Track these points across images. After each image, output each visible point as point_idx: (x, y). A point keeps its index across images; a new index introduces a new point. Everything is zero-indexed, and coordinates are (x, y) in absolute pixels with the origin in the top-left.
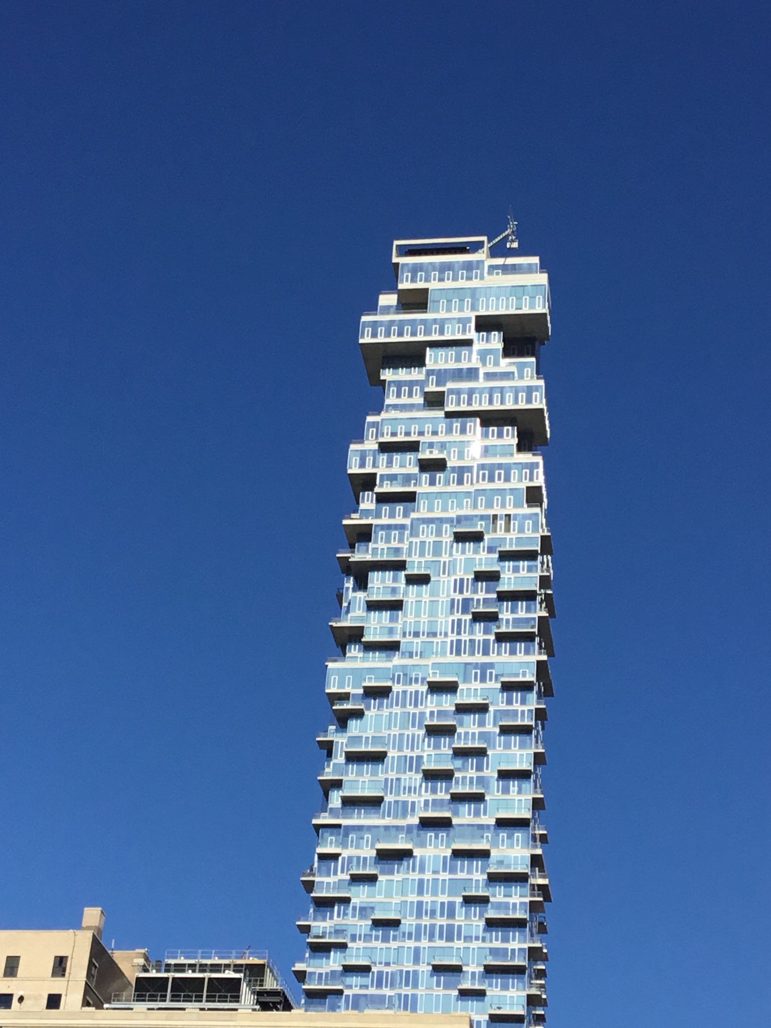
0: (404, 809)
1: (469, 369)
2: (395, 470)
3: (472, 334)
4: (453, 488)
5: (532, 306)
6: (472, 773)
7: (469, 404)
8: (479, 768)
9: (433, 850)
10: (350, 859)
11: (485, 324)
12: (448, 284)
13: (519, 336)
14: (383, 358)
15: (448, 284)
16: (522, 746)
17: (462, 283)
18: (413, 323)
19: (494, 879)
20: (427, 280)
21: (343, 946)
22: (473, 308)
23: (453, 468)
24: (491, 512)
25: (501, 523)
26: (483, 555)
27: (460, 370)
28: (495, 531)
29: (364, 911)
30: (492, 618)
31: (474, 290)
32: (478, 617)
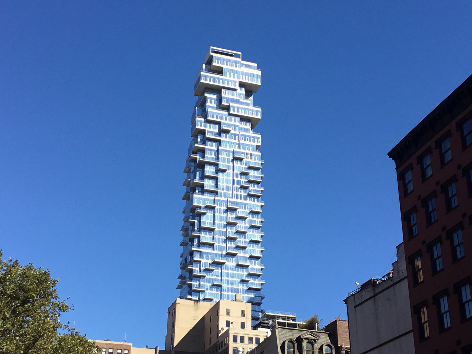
0: (220, 248)
1: (237, 100)
2: (212, 130)
3: (237, 87)
4: (232, 140)
5: (257, 82)
6: (242, 239)
7: (238, 112)
8: (245, 238)
9: (230, 263)
10: (205, 263)
11: (242, 85)
12: (229, 67)
13: (250, 90)
15: (229, 67)
16: (257, 233)
17: (233, 68)
18: (218, 79)
19: (250, 275)
20: (223, 64)
21: (204, 291)
22: (238, 78)
23: (232, 134)
24: (245, 151)
25: (249, 156)
26: (244, 166)
27: (233, 99)
28: (247, 158)
29: (210, 280)
30: (246, 188)
31: (237, 71)
32: (242, 187)
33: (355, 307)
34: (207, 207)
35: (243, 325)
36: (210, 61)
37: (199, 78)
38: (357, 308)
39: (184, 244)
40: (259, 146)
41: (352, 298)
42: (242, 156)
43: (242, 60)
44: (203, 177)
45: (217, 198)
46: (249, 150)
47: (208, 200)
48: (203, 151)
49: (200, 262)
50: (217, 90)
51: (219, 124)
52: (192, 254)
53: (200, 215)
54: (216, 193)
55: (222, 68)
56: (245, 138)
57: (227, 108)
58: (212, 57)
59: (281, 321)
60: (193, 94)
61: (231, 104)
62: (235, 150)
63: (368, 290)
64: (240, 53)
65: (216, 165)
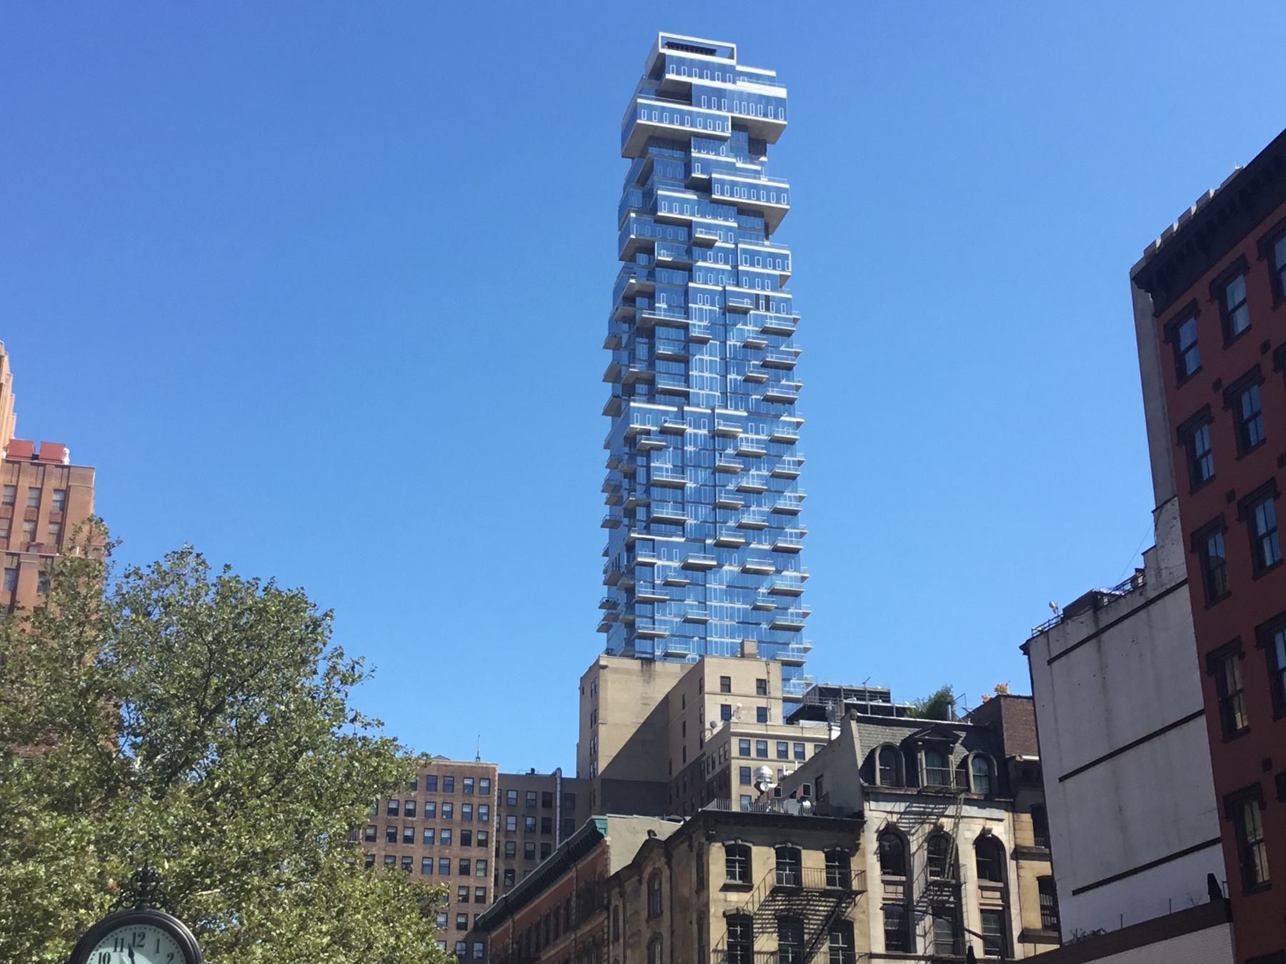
14: (650, 138)
20: (690, 75)
23: (721, 249)
25: (762, 302)
33: (1050, 662)
34: (664, 431)
35: (762, 715)
36: (660, 67)
37: (634, 112)
38: (1055, 664)
39: (610, 524)
40: (787, 277)
41: (1042, 640)
42: (746, 304)
43: (738, 63)
44: (653, 358)
45: (686, 408)
46: (763, 289)
47: (666, 413)
49: (652, 565)
50: (682, 143)
51: (689, 225)
52: (631, 547)
53: (647, 453)
54: (686, 395)
55: (690, 85)
56: (753, 257)
57: (704, 187)
58: (663, 56)
59: (854, 701)
60: (619, 153)
61: (714, 175)
62: (728, 288)
63: (1082, 618)
64: (733, 46)
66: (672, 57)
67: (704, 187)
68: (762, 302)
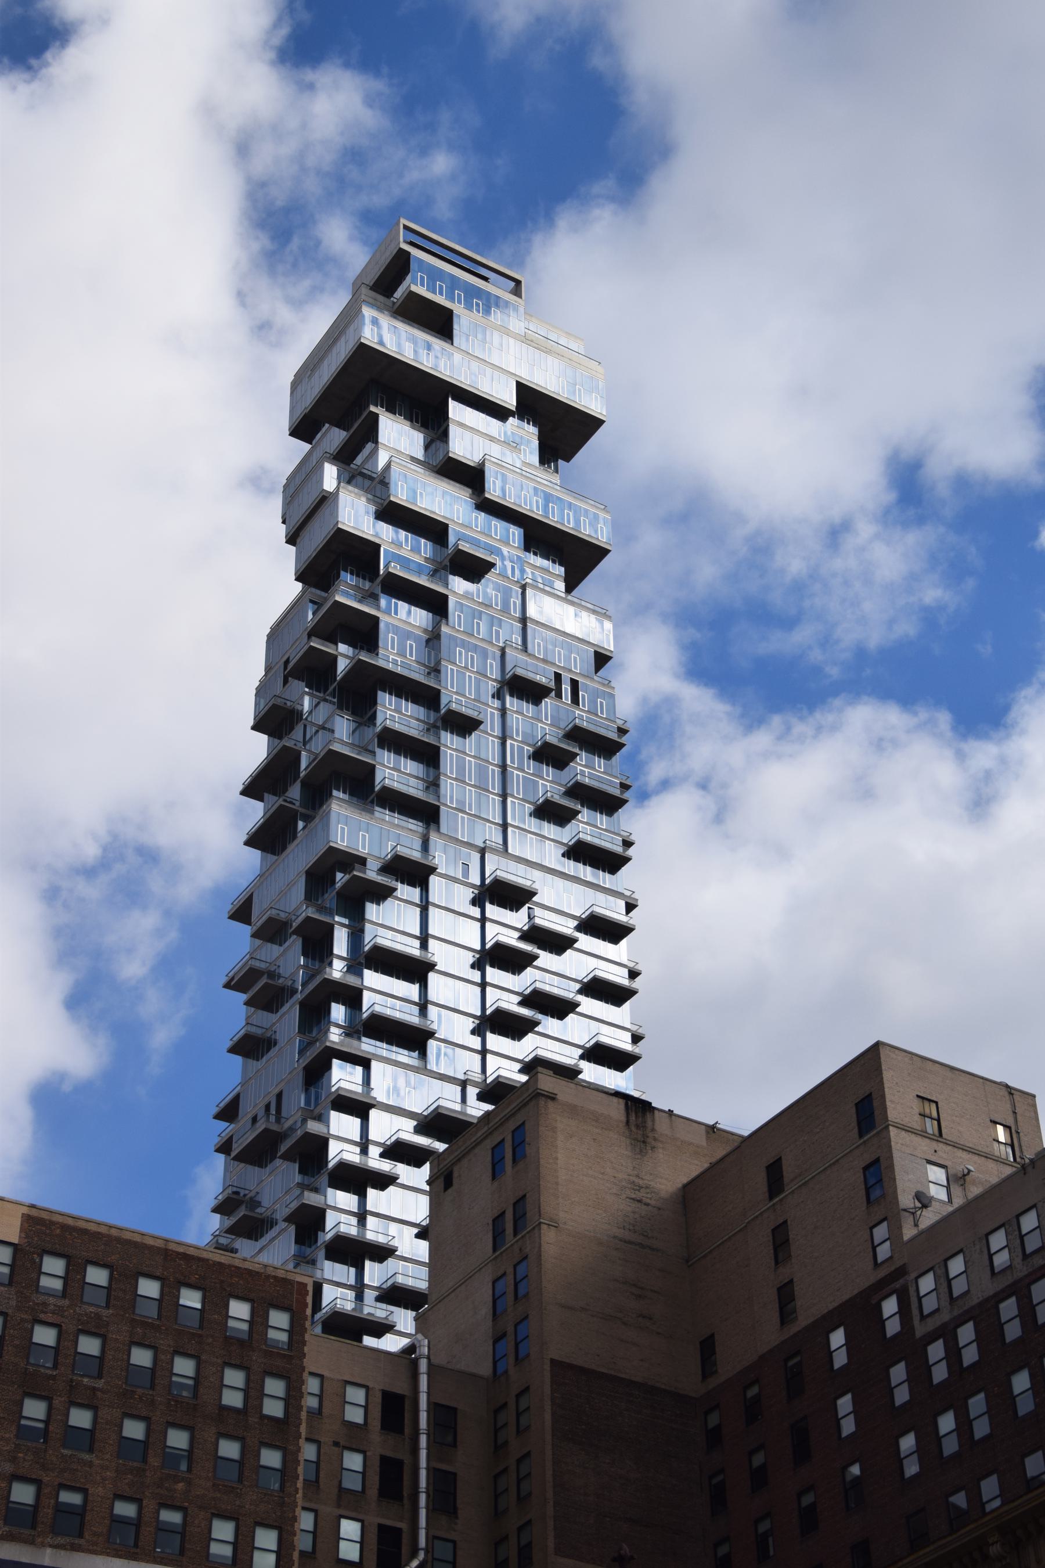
25: (566, 687)
28: (559, 695)
48: (365, 633)
65: (426, 696)
66: (420, 261)
67: (469, 477)
68: (566, 687)
